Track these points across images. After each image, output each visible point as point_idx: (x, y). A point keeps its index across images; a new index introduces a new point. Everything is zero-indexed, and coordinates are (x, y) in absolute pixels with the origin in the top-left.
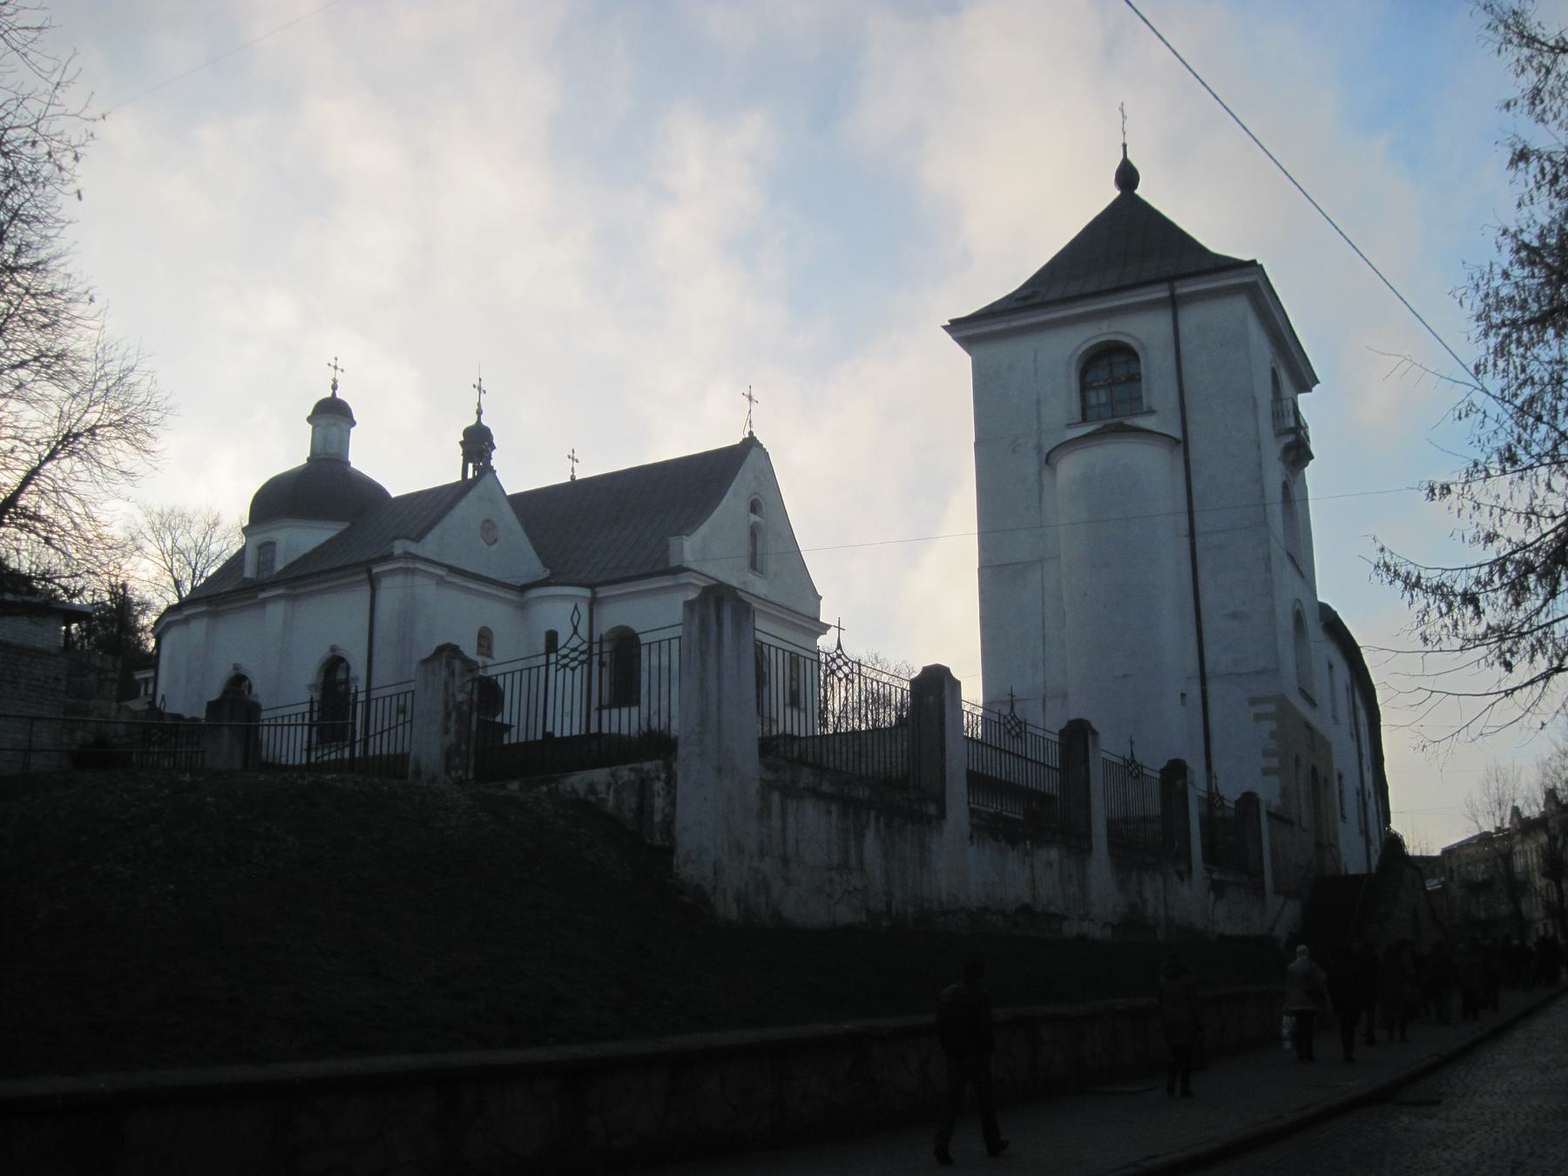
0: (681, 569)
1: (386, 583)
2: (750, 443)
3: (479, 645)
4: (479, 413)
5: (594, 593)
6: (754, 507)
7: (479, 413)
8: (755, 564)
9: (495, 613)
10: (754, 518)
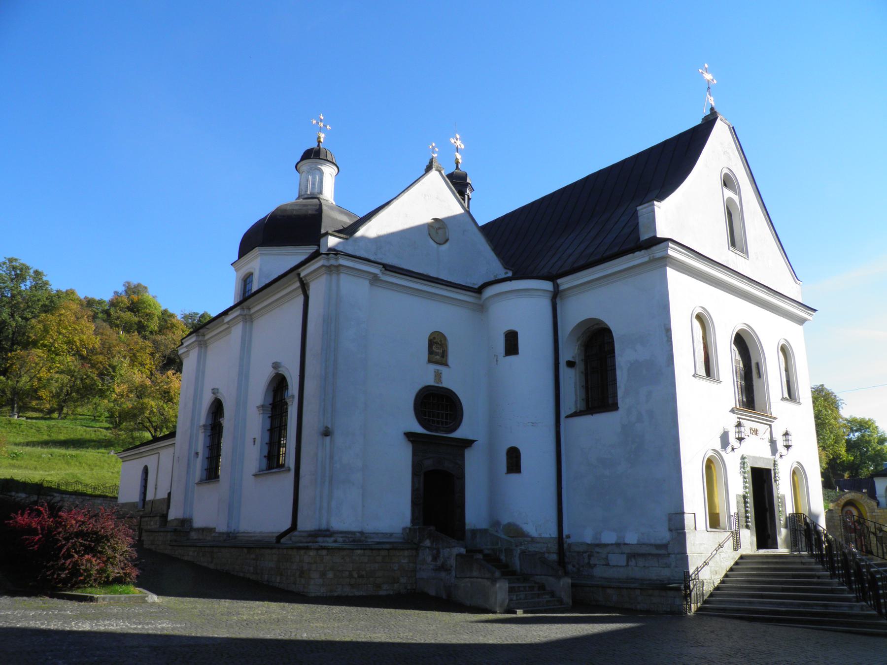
3: (431, 352)
5: (556, 286)
6: (728, 182)
8: (735, 241)
9: (445, 315)
10: (728, 193)
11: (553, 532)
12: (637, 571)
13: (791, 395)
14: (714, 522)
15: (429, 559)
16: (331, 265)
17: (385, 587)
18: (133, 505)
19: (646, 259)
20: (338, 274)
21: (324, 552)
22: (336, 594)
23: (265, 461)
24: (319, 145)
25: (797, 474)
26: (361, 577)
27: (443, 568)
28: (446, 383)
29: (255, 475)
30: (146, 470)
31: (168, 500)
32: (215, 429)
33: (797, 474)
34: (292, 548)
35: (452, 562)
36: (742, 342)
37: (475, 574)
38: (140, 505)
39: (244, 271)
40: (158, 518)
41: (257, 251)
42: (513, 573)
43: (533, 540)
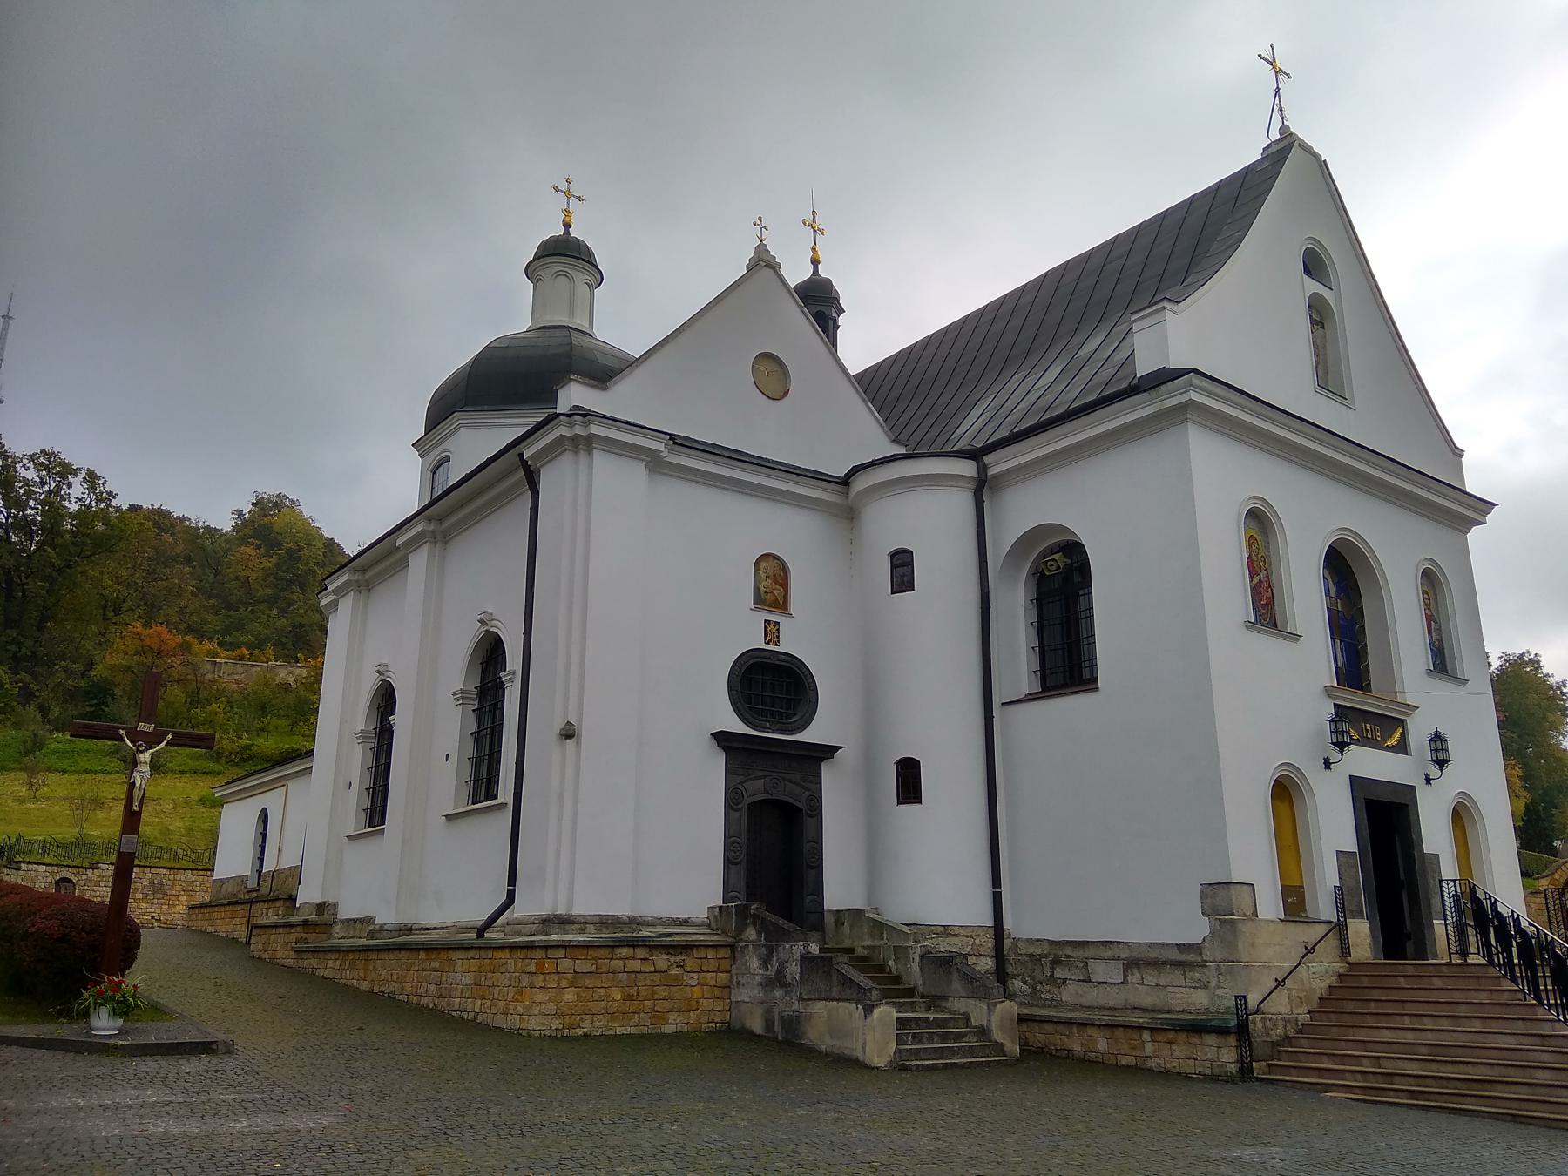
0: (1166, 376)
1: (548, 480)
2: (1285, 148)
4: (815, 262)
5: (982, 469)
6: (1314, 265)
7: (815, 262)
10: (1313, 287)
11: (982, 916)
12: (1144, 991)
13: (1441, 663)
14: (1295, 902)
15: (755, 964)
16: (576, 437)
17: (673, 1017)
18: (242, 880)
19: (1149, 410)
20: (589, 452)
21: (561, 953)
22: (580, 1032)
23: (465, 792)
24: (567, 232)
25: (1462, 816)
26: (630, 998)
27: (779, 980)
28: (785, 647)
29: (449, 817)
30: (264, 817)
31: (296, 873)
32: (383, 738)
33: (1462, 816)
34: (502, 948)
35: (793, 969)
36: (1345, 569)
37: (835, 993)
38: (252, 884)
39: (434, 457)
40: (279, 903)
41: (458, 418)
42: (911, 992)
43: (946, 931)
